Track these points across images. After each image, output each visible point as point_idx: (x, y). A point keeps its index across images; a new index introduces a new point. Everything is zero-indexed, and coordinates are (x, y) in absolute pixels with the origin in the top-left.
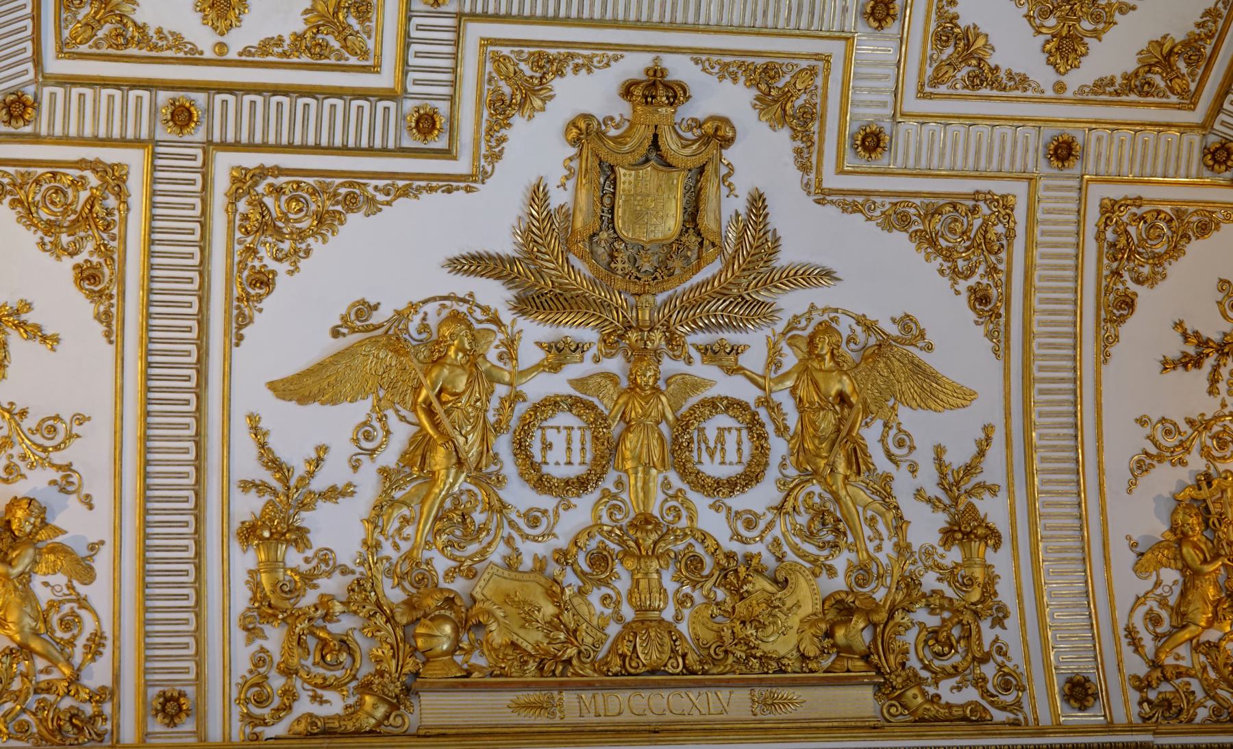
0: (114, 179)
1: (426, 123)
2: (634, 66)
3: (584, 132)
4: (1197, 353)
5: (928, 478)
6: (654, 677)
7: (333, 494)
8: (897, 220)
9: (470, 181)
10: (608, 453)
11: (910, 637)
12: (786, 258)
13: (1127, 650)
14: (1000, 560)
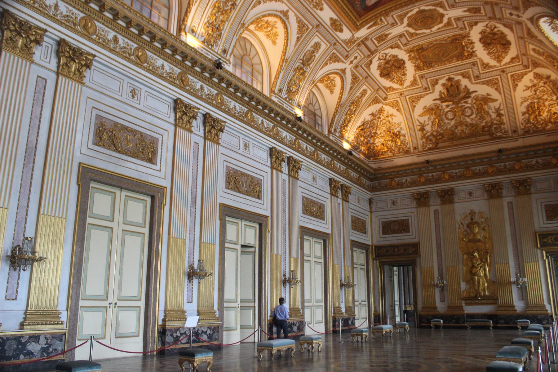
0: (397, 101)
1: (426, 89)
2: (447, 77)
3: (443, 85)
4: (528, 88)
5: (493, 110)
6: (463, 138)
7: (427, 125)
8: (483, 83)
9: (433, 92)
10: (455, 115)
11: (493, 129)
12: (471, 91)
13: (521, 125)
14: (504, 118)
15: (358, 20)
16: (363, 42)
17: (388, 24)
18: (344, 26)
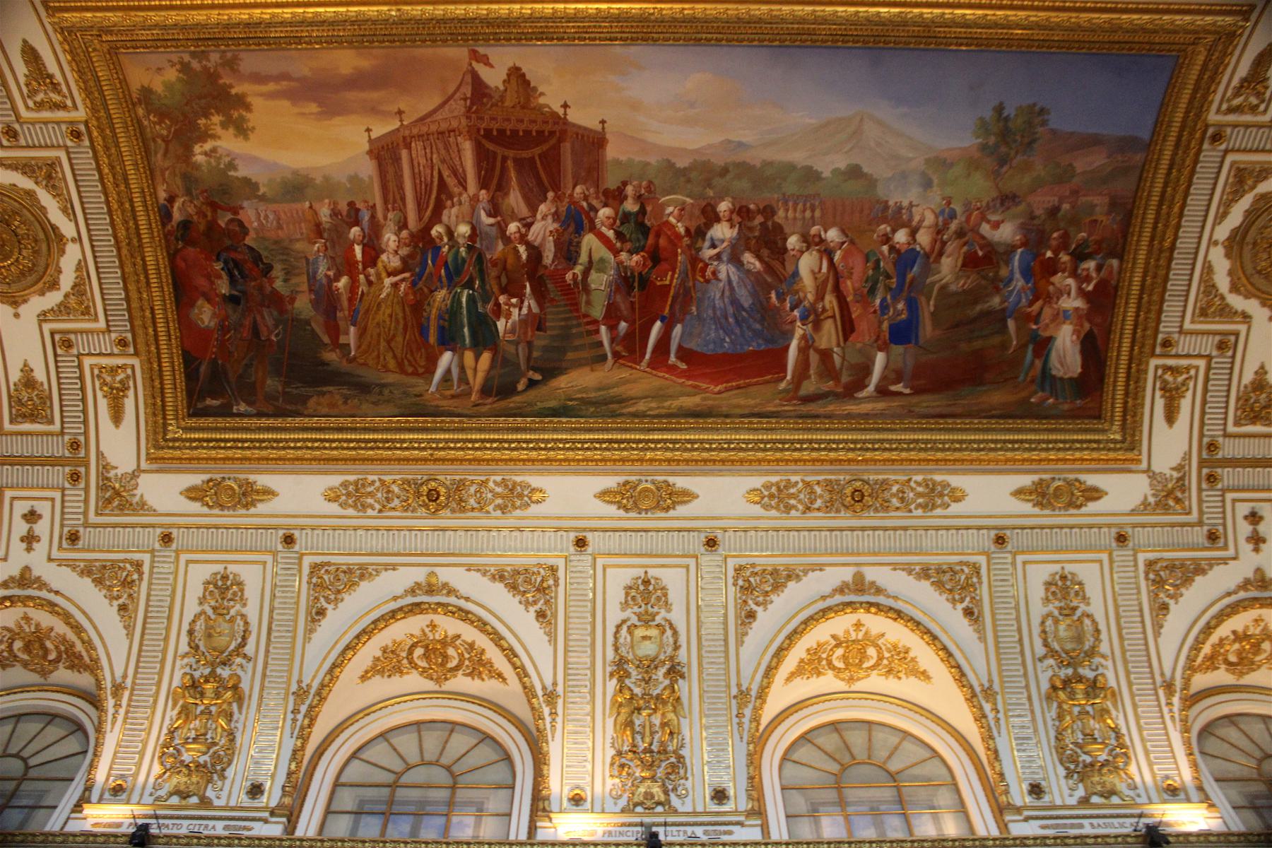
15: (1104, 431)
16: (1211, 460)
17: (1209, 358)
18: (1082, 477)
